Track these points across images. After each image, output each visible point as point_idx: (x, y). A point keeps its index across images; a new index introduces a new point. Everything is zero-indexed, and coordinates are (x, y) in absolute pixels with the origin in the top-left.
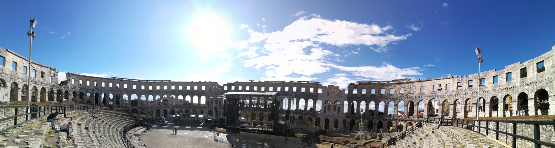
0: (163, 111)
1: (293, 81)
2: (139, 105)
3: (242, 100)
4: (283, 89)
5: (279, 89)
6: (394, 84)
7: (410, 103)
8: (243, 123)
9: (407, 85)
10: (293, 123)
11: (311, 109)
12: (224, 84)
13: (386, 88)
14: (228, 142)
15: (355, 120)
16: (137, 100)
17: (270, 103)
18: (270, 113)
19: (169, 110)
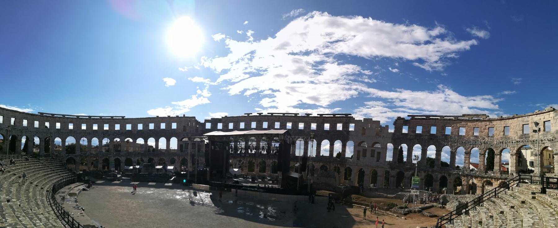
0: (114, 160)
1: (311, 114)
2: (78, 153)
3: (233, 143)
4: (295, 125)
5: (289, 125)
6: (466, 120)
7: (487, 151)
8: (236, 176)
9: (483, 123)
10: (312, 175)
11: (338, 154)
12: (205, 120)
13: (453, 126)
14: (213, 205)
15: (405, 172)
16: (75, 144)
17: (276, 146)
18: (276, 161)
19: (123, 159)
